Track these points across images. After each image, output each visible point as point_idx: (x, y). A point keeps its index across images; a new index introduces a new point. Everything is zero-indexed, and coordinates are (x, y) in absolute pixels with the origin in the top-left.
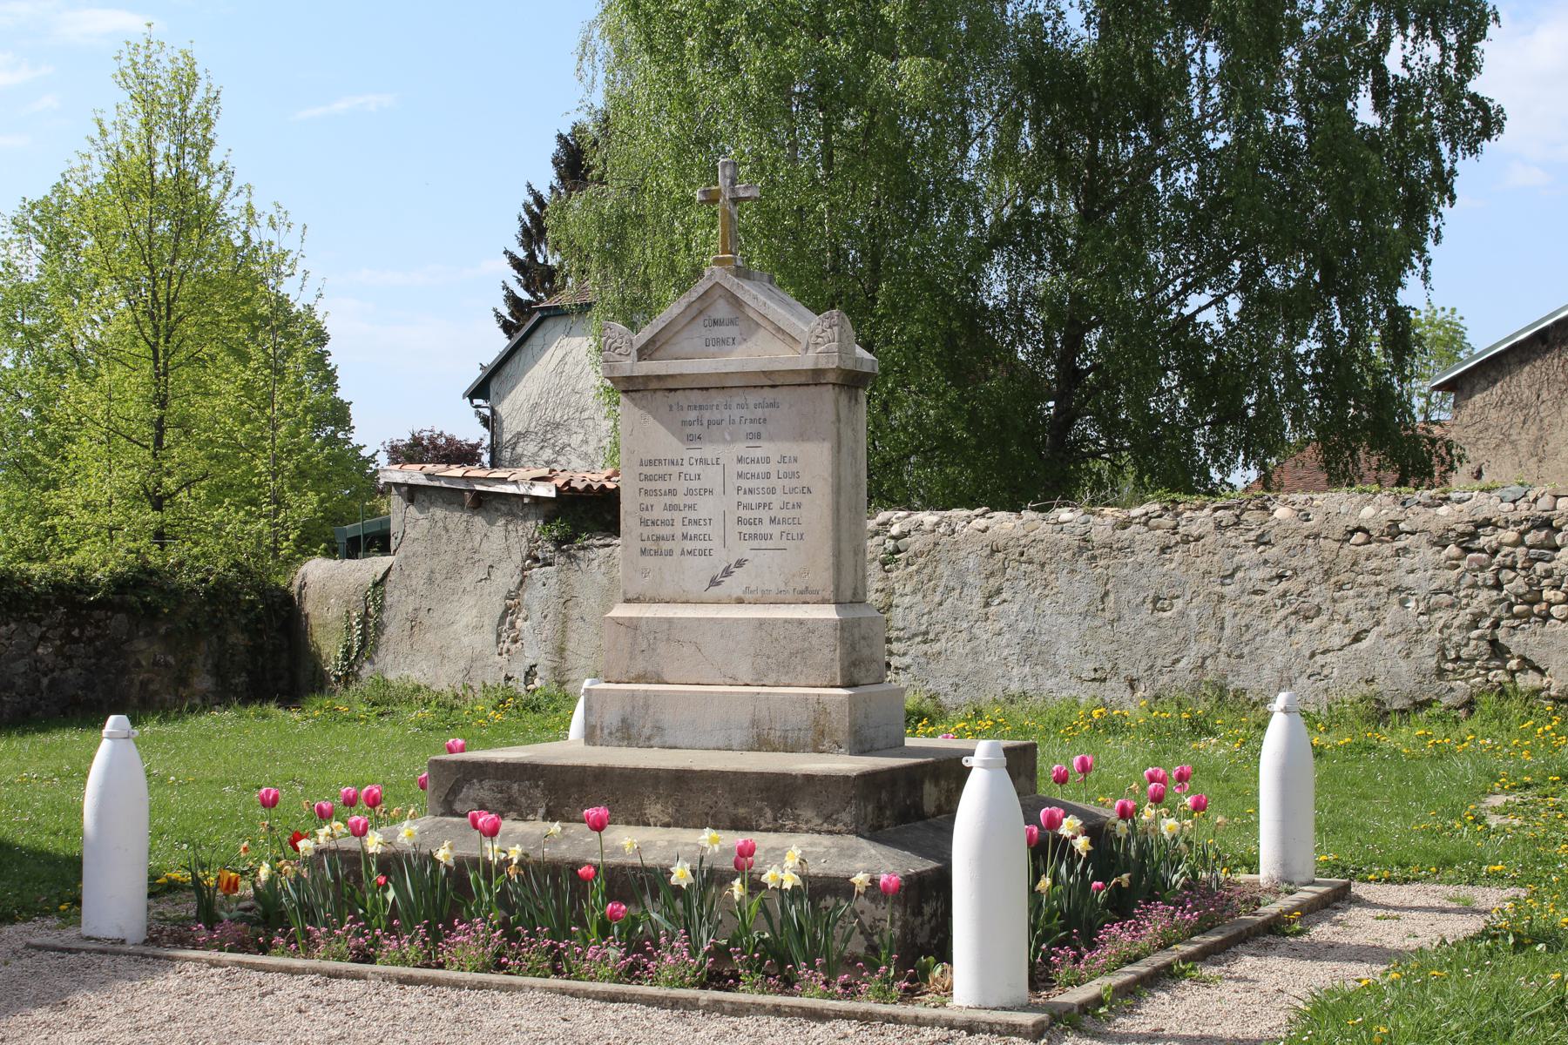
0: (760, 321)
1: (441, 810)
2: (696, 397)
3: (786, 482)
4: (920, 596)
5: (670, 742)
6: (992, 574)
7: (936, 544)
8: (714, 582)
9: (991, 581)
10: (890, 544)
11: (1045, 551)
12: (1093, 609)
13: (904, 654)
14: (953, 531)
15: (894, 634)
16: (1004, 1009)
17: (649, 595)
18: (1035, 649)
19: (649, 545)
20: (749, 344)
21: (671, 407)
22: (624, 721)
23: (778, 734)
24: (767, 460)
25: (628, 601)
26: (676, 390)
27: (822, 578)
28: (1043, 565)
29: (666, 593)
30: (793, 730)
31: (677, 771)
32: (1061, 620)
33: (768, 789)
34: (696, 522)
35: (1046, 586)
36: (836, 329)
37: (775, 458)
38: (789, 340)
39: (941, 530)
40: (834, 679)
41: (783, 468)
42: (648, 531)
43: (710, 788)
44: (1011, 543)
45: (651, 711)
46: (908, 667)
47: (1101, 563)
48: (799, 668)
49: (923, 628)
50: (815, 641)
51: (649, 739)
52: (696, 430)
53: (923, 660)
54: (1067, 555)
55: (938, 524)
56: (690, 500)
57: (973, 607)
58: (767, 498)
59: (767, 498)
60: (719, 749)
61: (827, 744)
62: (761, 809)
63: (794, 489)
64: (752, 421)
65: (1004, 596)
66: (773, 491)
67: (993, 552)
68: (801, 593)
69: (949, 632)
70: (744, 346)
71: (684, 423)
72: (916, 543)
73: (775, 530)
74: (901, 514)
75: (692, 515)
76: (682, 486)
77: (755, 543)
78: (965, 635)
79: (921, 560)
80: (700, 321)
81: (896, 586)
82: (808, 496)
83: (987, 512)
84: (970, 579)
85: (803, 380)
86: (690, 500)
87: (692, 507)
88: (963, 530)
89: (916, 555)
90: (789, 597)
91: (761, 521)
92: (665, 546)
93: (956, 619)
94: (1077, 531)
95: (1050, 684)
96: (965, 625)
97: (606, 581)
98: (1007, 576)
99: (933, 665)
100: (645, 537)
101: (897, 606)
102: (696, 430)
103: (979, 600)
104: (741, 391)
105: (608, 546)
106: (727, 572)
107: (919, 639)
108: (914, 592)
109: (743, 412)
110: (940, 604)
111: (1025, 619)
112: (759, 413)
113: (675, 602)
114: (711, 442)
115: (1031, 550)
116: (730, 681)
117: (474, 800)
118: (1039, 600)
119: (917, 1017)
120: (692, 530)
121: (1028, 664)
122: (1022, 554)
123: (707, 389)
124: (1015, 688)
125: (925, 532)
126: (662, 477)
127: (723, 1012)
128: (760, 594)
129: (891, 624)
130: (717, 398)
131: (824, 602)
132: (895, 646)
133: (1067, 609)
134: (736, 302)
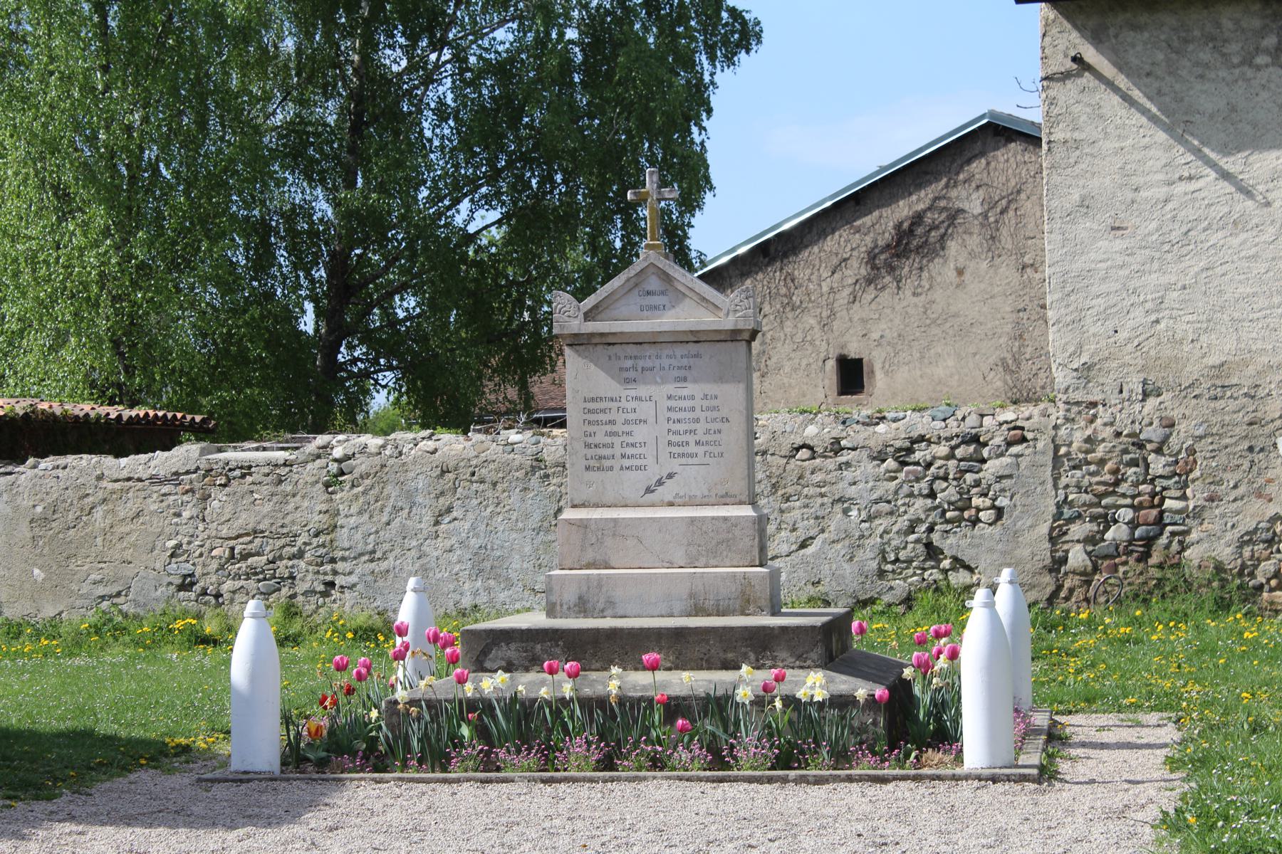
0: (687, 292)
1: (474, 668)
2: (632, 350)
3: (709, 414)
4: (366, 516)
5: (621, 612)
6: (442, 493)
7: (383, 466)
8: (649, 490)
9: (441, 500)
10: (334, 467)
11: (497, 471)
12: (546, 524)
13: (350, 573)
14: (401, 454)
15: (339, 554)
16: (1006, 767)
17: (593, 500)
18: (487, 565)
19: (592, 463)
20: (677, 309)
21: (610, 357)
22: (580, 598)
23: (712, 603)
24: (693, 398)
25: (574, 506)
26: (614, 344)
27: (738, 486)
28: (495, 484)
29: (609, 498)
30: (724, 599)
31: (676, 629)
32: (514, 535)
33: (751, 639)
34: (633, 445)
35: (499, 504)
36: (751, 299)
37: (699, 396)
38: (711, 307)
39: (388, 452)
40: (754, 560)
41: (706, 403)
42: (590, 452)
43: (703, 640)
44: (462, 464)
45: (604, 589)
46: (354, 585)
47: (554, 481)
48: (725, 553)
49: (370, 547)
50: (737, 532)
51: (602, 611)
52: (632, 374)
53: (370, 578)
54: (520, 474)
55: (384, 447)
56: (627, 428)
57: (422, 526)
58: (693, 426)
59: (693, 426)
60: (663, 616)
61: (752, 609)
62: (745, 654)
63: (715, 419)
64: (679, 368)
65: (454, 514)
66: (697, 420)
67: (443, 472)
68: (722, 497)
69: (398, 551)
70: (673, 311)
71: (621, 369)
72: (361, 465)
73: (700, 450)
74: (341, 437)
75: (630, 440)
76: (621, 418)
77: (683, 461)
78: (413, 553)
79: (368, 482)
80: (636, 292)
81: (341, 507)
82: (727, 425)
83: (433, 434)
84: (420, 499)
85: (722, 337)
86: (627, 428)
87: (629, 434)
88: (411, 453)
89: (362, 477)
90: (713, 500)
91: (687, 443)
92: (607, 463)
93: (404, 538)
94: (529, 452)
95: (502, 596)
96: (414, 543)
97: (9, 510)
98: (458, 495)
99: (380, 583)
100: (589, 457)
101: (342, 527)
102: (632, 374)
103: (428, 518)
104: (669, 345)
105: (10, 473)
106: (660, 483)
107: (366, 558)
108: (360, 513)
109: (673, 361)
110: (388, 524)
111: (477, 536)
112: (685, 362)
113: (616, 506)
114: (645, 383)
115: (483, 470)
116: (668, 565)
117: (502, 659)
118: (491, 518)
119: (954, 775)
120: (630, 451)
121: (480, 579)
122: (473, 474)
123: (641, 343)
124: (467, 602)
125: (370, 455)
126: (603, 411)
127: (808, 783)
128: (687, 499)
129: (335, 544)
130: (650, 351)
131: (741, 503)
132: (340, 566)
133: (520, 525)
134: (667, 278)
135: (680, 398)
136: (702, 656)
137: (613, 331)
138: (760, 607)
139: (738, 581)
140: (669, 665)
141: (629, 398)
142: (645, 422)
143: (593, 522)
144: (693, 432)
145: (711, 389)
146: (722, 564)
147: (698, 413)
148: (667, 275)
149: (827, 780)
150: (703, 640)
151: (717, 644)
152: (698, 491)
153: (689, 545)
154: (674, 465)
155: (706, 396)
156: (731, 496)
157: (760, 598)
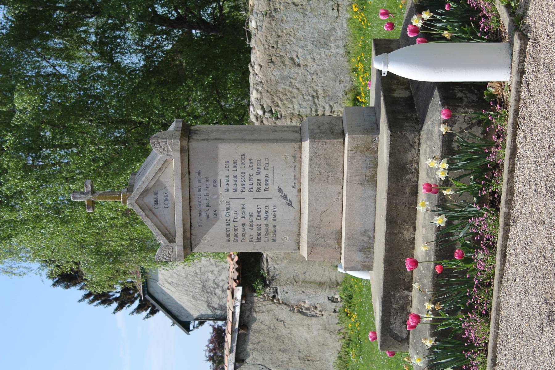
0: (155, 179)
1: (406, 344)
2: (195, 213)
3: (239, 166)
4: (294, 100)
5: (371, 227)
6: (283, 62)
7: (268, 91)
8: (290, 204)
9: (287, 63)
10: (268, 115)
11: (272, 35)
12: (301, 11)
13: (324, 108)
14: (261, 82)
15: (314, 113)
16: (512, 55)
17: (296, 237)
18: (322, 41)
19: (270, 237)
20: (167, 185)
21: (199, 226)
22: (360, 251)
23: (368, 171)
24: (227, 176)
25: (299, 248)
26: (191, 223)
27: (288, 148)
28: (279, 36)
29: (295, 228)
30: (366, 164)
31: (387, 223)
32: (307, 27)
33: (397, 176)
34: (259, 213)
35: (289, 34)
36: (160, 141)
37: (226, 172)
38: (165, 165)
39: (260, 89)
40: (340, 142)
41: (231, 168)
42: (263, 238)
43: (396, 206)
44: (267, 52)
45: (356, 236)
46: (331, 106)
47: (278, 6)
48: (334, 160)
49: (311, 98)
50: (320, 152)
51: (370, 238)
52: (211, 213)
53: (327, 99)
54: (274, 24)
55: (257, 90)
56: (248, 216)
57: (300, 72)
58: (247, 176)
59: (247, 176)
60: (375, 202)
61: (373, 146)
62: (407, 180)
63: (242, 163)
64: (207, 184)
65: (294, 56)
66: (243, 174)
67: (272, 62)
68: (295, 159)
69: (313, 85)
70: (168, 188)
71: (208, 219)
72: (267, 102)
73: (263, 172)
74: (252, 109)
75: (255, 215)
76: (240, 220)
77: (270, 183)
78: (315, 77)
79: (276, 99)
80: (155, 211)
81: (289, 112)
82: (246, 156)
83: (251, 65)
84: (286, 74)
85: (186, 158)
86: (248, 216)
87: (251, 215)
88: (260, 77)
89: (273, 102)
90: (298, 165)
91: (258, 180)
92: (271, 229)
93: (306, 81)
94: (262, 18)
95: (340, 33)
96: (309, 77)
97: (285, 261)
98: (284, 55)
99: (330, 93)
100: (266, 239)
101: (299, 112)
102: (211, 213)
103: (296, 69)
104: (191, 190)
105: (267, 260)
106: (285, 197)
107: (316, 100)
108: (292, 103)
109: (203, 188)
110: (298, 89)
111: (306, 46)
112: (203, 180)
113: (300, 224)
114: (218, 205)
115: (271, 42)
116: (341, 196)
117: (401, 327)
118: (297, 38)
119: (516, 100)
120: (263, 215)
121: (330, 44)
122: (273, 47)
123: (190, 207)
124: (341, 51)
125: (261, 97)
126: (236, 230)
127: (512, 200)
128: (296, 181)
129: (308, 115)
130: (195, 202)
131: (300, 147)
132: (320, 113)
133: (301, 24)
134: (146, 192)
135: (227, 184)
136: (407, 208)
137: (182, 226)
138: (373, 142)
139: (354, 155)
140: (412, 228)
141: (227, 215)
142: (243, 205)
143: (310, 240)
144: (251, 177)
145: (222, 164)
146: (342, 162)
147: (238, 173)
148: (144, 192)
149: (511, 187)
150: (396, 206)
151: (400, 198)
152: (291, 174)
153: (327, 182)
154: (273, 189)
155: (227, 168)
156: (295, 153)
157: (366, 141)
